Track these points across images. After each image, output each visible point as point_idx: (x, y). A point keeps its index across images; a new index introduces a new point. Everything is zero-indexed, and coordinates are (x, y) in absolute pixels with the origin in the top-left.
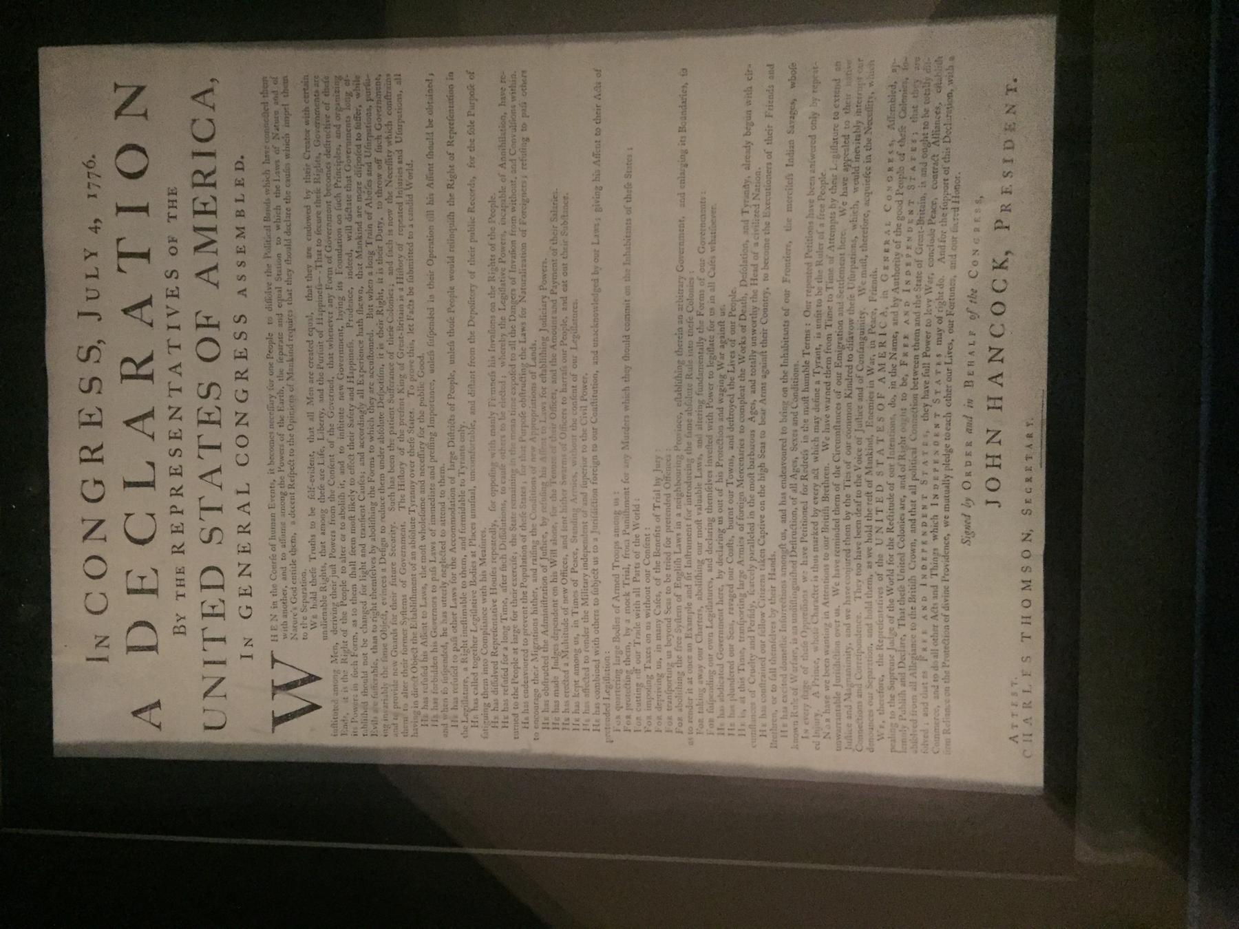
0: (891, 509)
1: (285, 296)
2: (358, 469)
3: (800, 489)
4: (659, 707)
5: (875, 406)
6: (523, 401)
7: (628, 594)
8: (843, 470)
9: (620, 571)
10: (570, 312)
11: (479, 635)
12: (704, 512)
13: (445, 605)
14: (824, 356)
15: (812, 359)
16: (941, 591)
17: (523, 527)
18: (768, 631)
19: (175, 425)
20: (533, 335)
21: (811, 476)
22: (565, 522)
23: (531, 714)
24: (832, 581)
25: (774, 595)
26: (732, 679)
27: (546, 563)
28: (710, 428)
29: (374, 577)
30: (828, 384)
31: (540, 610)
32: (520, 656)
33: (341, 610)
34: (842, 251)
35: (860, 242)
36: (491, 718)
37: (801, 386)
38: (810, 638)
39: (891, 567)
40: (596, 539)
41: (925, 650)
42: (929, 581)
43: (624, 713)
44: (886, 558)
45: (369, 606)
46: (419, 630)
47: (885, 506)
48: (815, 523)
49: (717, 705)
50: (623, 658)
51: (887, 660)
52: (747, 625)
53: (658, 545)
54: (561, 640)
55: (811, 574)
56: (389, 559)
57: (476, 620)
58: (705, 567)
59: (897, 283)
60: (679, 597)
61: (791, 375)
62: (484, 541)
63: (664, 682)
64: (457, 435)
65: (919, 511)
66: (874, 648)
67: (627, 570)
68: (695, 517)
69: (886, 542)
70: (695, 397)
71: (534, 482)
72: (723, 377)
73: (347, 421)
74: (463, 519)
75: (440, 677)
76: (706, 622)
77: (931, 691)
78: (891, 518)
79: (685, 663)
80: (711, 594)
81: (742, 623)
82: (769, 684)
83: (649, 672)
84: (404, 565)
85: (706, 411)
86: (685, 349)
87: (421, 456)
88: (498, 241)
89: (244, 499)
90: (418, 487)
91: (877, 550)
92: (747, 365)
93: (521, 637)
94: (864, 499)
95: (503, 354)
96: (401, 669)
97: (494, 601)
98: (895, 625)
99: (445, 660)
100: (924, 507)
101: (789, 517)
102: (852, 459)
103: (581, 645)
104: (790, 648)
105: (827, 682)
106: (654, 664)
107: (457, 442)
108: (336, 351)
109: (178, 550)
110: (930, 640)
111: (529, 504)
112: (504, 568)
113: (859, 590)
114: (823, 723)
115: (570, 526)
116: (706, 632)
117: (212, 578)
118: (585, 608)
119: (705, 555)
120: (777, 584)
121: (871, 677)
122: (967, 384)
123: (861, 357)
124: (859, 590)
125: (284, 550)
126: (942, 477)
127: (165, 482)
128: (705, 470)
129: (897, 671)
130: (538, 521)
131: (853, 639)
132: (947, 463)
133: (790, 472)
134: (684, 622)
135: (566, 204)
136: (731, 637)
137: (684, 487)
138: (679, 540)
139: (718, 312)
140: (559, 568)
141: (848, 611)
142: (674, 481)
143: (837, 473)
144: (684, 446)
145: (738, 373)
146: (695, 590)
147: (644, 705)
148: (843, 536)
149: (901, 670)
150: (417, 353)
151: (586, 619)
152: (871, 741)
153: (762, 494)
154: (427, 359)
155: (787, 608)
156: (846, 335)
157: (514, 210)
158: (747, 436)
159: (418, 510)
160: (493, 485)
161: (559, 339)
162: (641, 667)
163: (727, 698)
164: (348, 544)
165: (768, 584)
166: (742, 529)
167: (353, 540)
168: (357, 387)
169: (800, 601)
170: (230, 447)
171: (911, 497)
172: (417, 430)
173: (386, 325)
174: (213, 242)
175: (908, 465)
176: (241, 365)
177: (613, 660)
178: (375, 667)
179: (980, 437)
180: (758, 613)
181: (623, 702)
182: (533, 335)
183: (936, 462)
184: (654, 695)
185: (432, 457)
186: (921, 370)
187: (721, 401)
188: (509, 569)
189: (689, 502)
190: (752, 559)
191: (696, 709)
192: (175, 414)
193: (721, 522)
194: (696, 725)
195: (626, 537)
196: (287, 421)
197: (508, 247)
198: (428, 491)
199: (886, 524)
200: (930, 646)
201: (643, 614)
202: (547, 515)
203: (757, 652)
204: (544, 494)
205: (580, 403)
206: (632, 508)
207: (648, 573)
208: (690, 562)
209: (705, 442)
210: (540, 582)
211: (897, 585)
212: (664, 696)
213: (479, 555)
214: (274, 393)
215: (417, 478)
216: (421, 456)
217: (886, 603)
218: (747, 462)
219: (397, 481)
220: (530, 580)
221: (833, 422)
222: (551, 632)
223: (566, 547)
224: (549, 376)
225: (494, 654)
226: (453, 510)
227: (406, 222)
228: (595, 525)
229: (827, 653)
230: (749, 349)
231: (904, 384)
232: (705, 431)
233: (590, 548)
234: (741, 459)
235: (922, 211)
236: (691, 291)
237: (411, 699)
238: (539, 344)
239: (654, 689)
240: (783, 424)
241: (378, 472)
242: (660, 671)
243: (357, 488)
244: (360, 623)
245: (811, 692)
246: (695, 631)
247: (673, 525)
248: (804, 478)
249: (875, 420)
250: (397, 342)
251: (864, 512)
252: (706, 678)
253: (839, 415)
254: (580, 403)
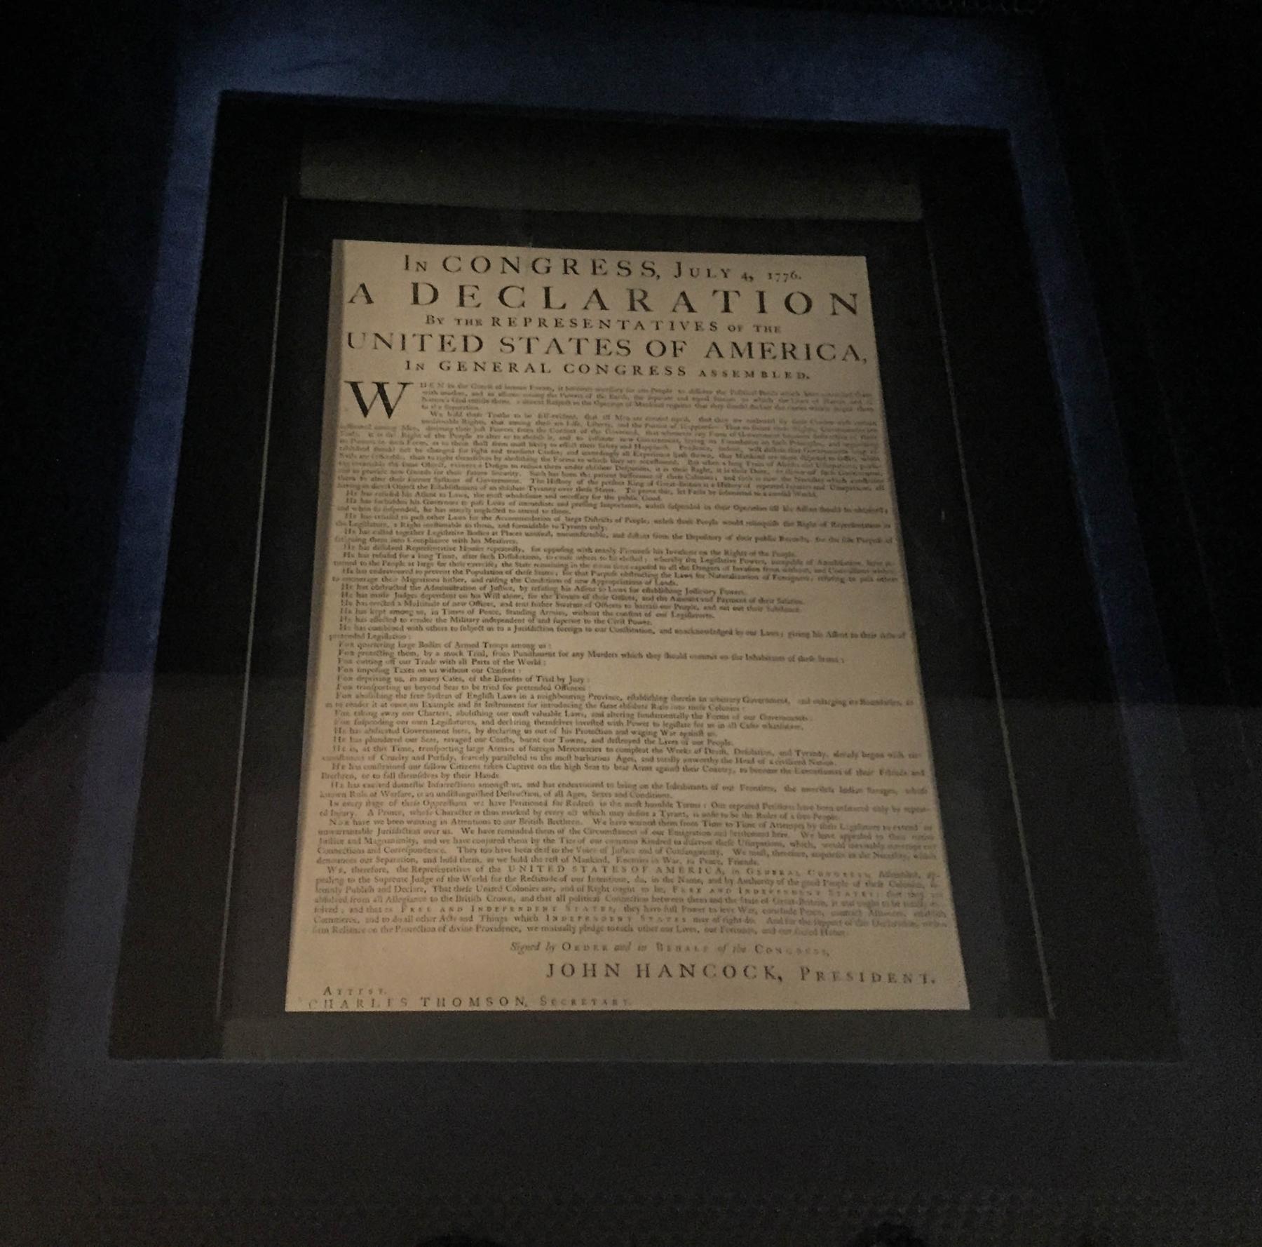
0: (542, 879)
1: (703, 403)
2: (564, 450)
3: (559, 799)
4: (359, 679)
5: (635, 864)
6: (626, 574)
7: (461, 654)
8: (575, 837)
9: (481, 648)
10: (702, 612)
11: (425, 537)
12: (536, 718)
13: (451, 510)
14: (678, 819)
15: (675, 809)
16: (468, 924)
17: (519, 572)
18: (428, 771)
19: (596, 323)
20: (682, 584)
21: (570, 808)
22: (524, 605)
23: (354, 575)
24: (474, 827)
25: (463, 776)
26: (386, 740)
27: (488, 590)
28: (609, 724)
29: (475, 458)
30: (653, 823)
31: (447, 584)
32: (407, 568)
33: (447, 433)
34: (771, 834)
35: (780, 849)
36: (352, 544)
37: (651, 801)
38: (423, 808)
39: (489, 879)
40: (509, 629)
41: (412, 910)
42: (476, 915)
43: (356, 650)
44: (497, 875)
45: (449, 454)
46: (429, 491)
47: (545, 873)
48: (527, 813)
49: (361, 727)
50: (405, 650)
51: (403, 875)
52: (434, 753)
53: (505, 679)
54: (420, 600)
55: (481, 809)
56: (489, 470)
57: (439, 534)
58: (486, 718)
59: (746, 882)
60: (459, 696)
61: (659, 791)
62: (508, 542)
64: (595, 524)
65: (541, 904)
66: (414, 864)
67: (483, 654)
68: (531, 710)
69: (512, 875)
70: (635, 711)
71: (558, 581)
72: (655, 734)
73: (604, 443)
74: (526, 527)
75: (389, 506)
76: (437, 719)
77: (374, 915)
78: (534, 879)
79: (399, 701)
80: (463, 723)
81: (436, 749)
82: (381, 772)
83: (392, 671)
84: (485, 481)
85: (624, 720)
86: (677, 703)
87: (576, 497)
88: (758, 557)
89: (537, 367)
90: (549, 493)
91: (504, 867)
92: (666, 754)
93: (423, 569)
94: (552, 855)
95: (664, 560)
96: (397, 476)
97: (454, 549)
98: (434, 883)
99: (402, 510)
100: (545, 909)
101: (532, 790)
102: (587, 845)
103: (416, 616)
104: (414, 791)
105: (382, 822)
106: (399, 675)
107: (589, 524)
108: (660, 437)
109: (496, 322)
110: (421, 915)
111: (538, 577)
112: (483, 557)
113: (467, 851)
114: (343, 819)
115: (520, 609)
116: (429, 719)
117: (473, 343)
118: (449, 620)
119: (497, 719)
120: (472, 780)
121: (387, 861)
122: (659, 946)
123: (679, 852)
124: (467, 851)
125: (496, 394)
126: (572, 924)
127: (550, 315)
128: (573, 719)
129: (393, 884)
130: (523, 584)
131: (421, 846)
132: (585, 928)
133: (573, 790)
134: (437, 701)
135: (791, 610)
136: (423, 740)
137: (556, 701)
138: (510, 697)
139: (710, 730)
140: (483, 599)
141: (448, 841)
142: (562, 693)
143: (574, 831)
144: (593, 701)
145: (659, 747)
146: (466, 710)
147: (362, 666)
148: (516, 837)
149: (393, 889)
150: (662, 496)
151: (439, 620)
152: (328, 861)
153: (553, 767)
154: (657, 503)
155: (450, 788)
156: (697, 838)
157: (785, 571)
158: (604, 754)
159: (532, 493)
160: (553, 550)
161: (682, 604)
162: (397, 664)
163: (367, 736)
164: (502, 440)
165: (472, 772)
166: (521, 750)
167: (505, 444)
168: (631, 451)
169: (456, 799)
170: (578, 361)
171: (554, 896)
172: (598, 494)
173: (683, 474)
174: (741, 355)
175: (584, 894)
176: (645, 370)
177: (403, 642)
178: (398, 457)
179: (612, 958)
180: (446, 763)
181: (364, 649)
182: (682, 584)
183: (587, 918)
185: (576, 505)
186: (670, 904)
187: (634, 733)
188: (483, 561)
189: (543, 706)
190: (494, 758)
191: (358, 709)
192: (604, 324)
193: (526, 732)
194: (344, 709)
195: (512, 654)
196: (601, 401)
197: (754, 565)
198: (547, 501)
199: (528, 874)
200: (416, 914)
201: (445, 666)
202: (529, 591)
203: (411, 762)
204: (546, 589)
205: (626, 619)
206: (537, 658)
207: (481, 671)
208: (491, 705)
209: (598, 719)
210: (470, 584)
211: (472, 885)
212: (370, 683)
213: (495, 538)
214: (624, 392)
215: (559, 494)
216: (576, 497)
217: (456, 875)
218: (580, 754)
219: (555, 478)
220: (473, 577)
221: (621, 827)
222: (427, 592)
223: (502, 605)
224: (648, 595)
225: (408, 548)
226: (533, 519)
227: (767, 491)
228: (520, 629)
229: (409, 822)
230: (681, 756)
231: (657, 890)
232: (606, 720)
233: (501, 625)
234: (583, 750)
235: (811, 902)
236: (727, 709)
237: (370, 483)
238: (674, 587)
239: (377, 675)
240: (616, 785)
241: (563, 464)
242: (392, 680)
243: (549, 449)
244: (435, 447)
245: (371, 807)
246: (429, 710)
247: (522, 692)
248: (568, 803)
249: (623, 864)
250: (671, 481)
251: (539, 855)
252: (387, 718)
253: (624, 832)
254: (626, 619)
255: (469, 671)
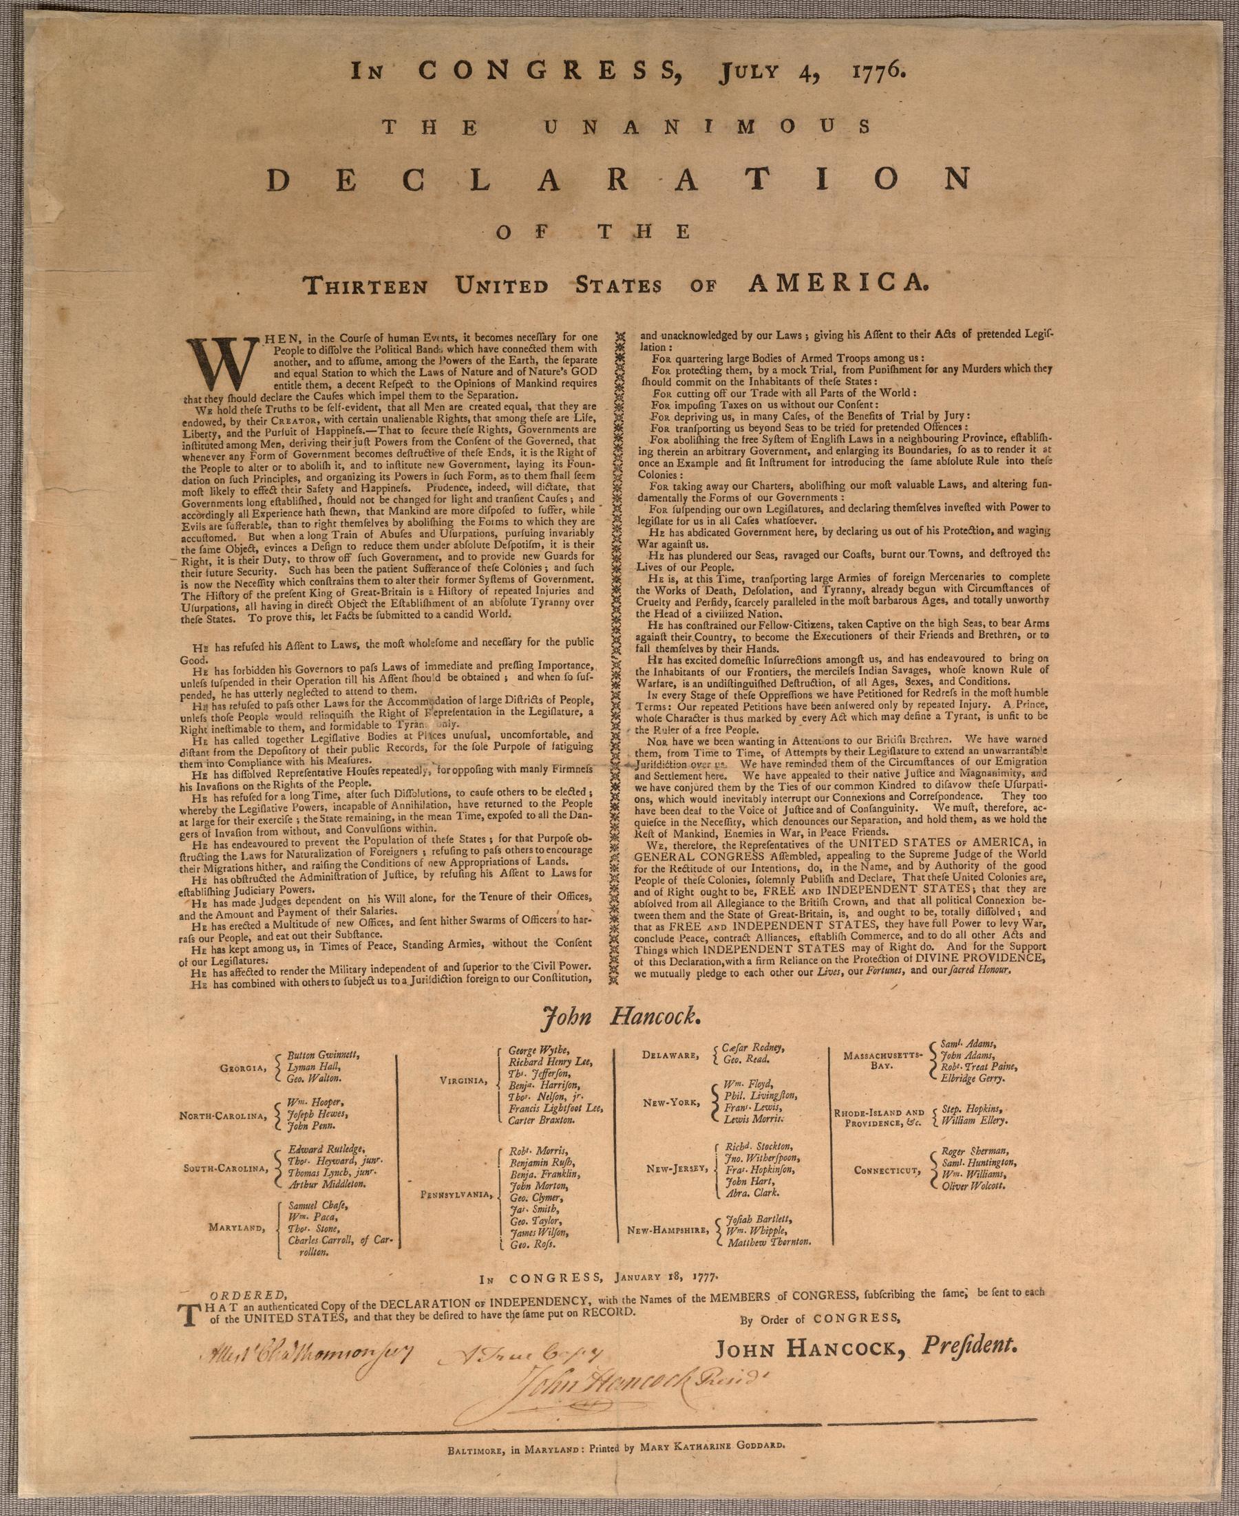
53: (861, 417)
63: (709, 424)
83: (719, 407)
147: (682, 400)
184: (692, 412)
207: (830, 405)
212: (691, 424)
239: (700, 412)
242: (720, 418)
255: (816, 405)
